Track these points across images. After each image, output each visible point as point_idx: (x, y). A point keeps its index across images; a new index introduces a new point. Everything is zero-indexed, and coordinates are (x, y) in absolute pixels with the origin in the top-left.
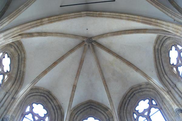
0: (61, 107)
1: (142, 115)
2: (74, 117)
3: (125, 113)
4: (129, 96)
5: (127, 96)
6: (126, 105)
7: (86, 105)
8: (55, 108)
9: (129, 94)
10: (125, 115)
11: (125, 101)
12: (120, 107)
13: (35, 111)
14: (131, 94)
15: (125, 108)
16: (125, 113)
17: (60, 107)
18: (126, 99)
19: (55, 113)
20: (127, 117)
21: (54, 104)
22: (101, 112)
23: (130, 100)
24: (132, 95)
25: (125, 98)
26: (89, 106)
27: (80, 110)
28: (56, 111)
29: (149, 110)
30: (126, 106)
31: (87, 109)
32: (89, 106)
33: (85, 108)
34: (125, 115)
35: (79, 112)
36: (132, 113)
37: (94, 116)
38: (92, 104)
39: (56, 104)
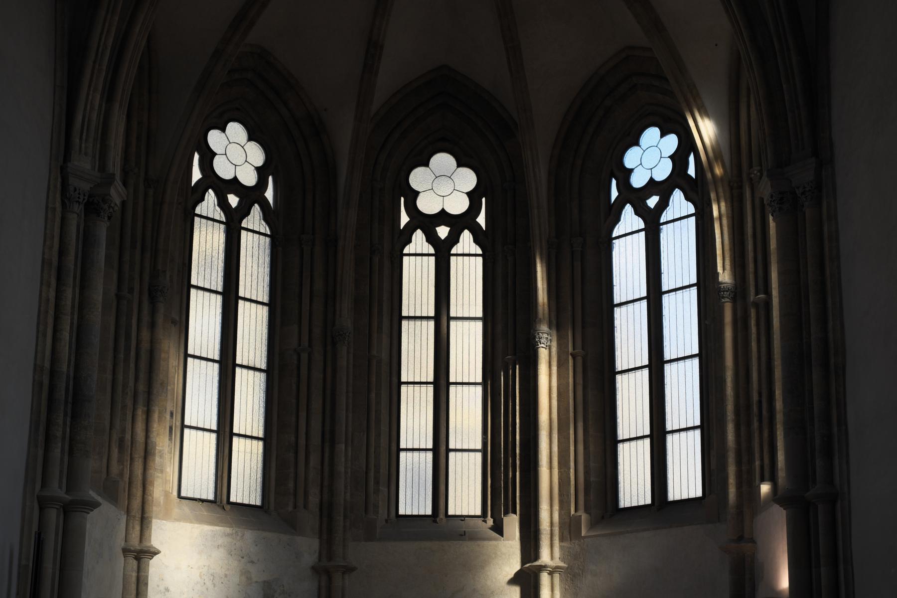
13: (223, 169)
29: (663, 189)
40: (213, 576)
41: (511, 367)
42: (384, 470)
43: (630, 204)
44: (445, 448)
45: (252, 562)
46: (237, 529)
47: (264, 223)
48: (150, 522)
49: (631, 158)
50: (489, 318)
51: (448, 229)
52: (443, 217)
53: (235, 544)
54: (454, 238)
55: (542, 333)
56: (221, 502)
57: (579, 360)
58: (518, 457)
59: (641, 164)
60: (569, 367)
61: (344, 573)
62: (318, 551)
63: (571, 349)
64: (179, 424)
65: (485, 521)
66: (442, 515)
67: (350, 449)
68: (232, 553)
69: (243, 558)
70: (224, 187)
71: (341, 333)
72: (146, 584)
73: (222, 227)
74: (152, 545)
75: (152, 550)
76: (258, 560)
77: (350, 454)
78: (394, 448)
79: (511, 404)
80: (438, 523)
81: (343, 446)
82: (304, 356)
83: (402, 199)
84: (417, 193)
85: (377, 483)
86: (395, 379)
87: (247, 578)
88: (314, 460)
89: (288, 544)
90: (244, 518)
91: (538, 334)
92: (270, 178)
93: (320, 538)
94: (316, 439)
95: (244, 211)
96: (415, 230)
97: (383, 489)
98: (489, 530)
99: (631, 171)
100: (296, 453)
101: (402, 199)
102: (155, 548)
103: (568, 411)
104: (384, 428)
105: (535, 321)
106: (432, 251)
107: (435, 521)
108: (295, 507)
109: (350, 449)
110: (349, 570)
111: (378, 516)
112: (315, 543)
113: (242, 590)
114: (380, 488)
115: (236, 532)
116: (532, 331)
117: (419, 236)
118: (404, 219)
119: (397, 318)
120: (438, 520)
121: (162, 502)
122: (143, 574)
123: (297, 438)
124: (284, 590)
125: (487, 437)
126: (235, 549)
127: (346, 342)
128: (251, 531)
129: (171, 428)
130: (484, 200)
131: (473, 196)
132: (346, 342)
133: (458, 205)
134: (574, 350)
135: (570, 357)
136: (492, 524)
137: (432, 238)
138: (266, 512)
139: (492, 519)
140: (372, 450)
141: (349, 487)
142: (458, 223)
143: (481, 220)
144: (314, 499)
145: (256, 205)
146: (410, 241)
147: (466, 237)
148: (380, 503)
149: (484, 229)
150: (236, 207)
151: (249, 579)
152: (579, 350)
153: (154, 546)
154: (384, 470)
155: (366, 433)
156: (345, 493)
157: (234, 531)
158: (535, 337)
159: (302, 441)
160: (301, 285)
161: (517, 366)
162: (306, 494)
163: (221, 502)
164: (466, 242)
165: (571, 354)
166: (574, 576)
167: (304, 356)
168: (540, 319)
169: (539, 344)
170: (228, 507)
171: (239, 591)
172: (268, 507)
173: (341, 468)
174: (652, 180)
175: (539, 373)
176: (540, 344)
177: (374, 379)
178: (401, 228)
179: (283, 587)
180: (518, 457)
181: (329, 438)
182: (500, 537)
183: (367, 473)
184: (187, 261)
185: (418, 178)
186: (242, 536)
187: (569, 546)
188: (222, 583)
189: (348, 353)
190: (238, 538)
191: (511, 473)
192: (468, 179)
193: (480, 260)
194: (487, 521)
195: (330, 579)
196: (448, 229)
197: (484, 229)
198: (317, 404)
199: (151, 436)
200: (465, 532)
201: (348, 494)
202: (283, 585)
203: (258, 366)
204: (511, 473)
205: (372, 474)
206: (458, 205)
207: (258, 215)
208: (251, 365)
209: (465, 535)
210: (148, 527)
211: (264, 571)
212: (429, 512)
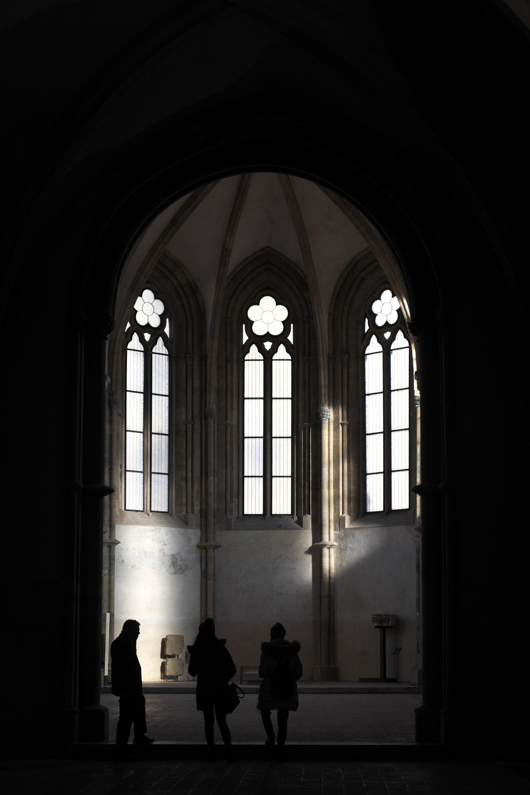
2: (228, 307)
40: (146, 553)
41: (307, 429)
42: (235, 489)
43: (375, 335)
44: (270, 475)
45: (165, 544)
46: (157, 527)
47: (165, 348)
48: (115, 527)
50: (295, 398)
51: (271, 344)
52: (268, 337)
53: (156, 535)
54: (274, 350)
55: (324, 412)
56: (147, 511)
57: (346, 427)
58: (311, 482)
59: (381, 312)
60: (339, 431)
61: (214, 549)
62: (200, 537)
63: (341, 421)
64: (123, 470)
65: (293, 518)
66: (268, 515)
67: (216, 479)
68: (155, 540)
69: (160, 542)
70: (141, 330)
71: (210, 413)
72: (114, 559)
73: (142, 353)
74: (116, 539)
75: (116, 542)
76: (168, 543)
77: (216, 481)
78: (241, 476)
79: (307, 451)
80: (266, 519)
81: (212, 478)
82: (190, 426)
83: (244, 325)
84: (252, 322)
85: (232, 497)
86: (241, 436)
87: (163, 553)
88: (196, 486)
89: (184, 534)
90: (160, 520)
91: (322, 412)
92: (167, 320)
93: (201, 529)
94: (197, 474)
95: (153, 342)
96: (251, 345)
97: (235, 500)
98: (295, 523)
99: (376, 315)
100: (186, 482)
101: (244, 325)
102: (118, 541)
103: (339, 456)
104: (235, 465)
105: (320, 404)
106: (262, 358)
107: (265, 518)
108: (187, 512)
109: (216, 479)
110: (217, 547)
111: (232, 516)
112: (198, 532)
113: (161, 560)
114: (234, 500)
115: (156, 529)
116: (319, 410)
117: (254, 349)
118: (245, 338)
119: (241, 398)
120: (266, 517)
121: (119, 515)
122: (112, 554)
123: (186, 473)
124: (182, 559)
125: (294, 469)
126: (156, 538)
127: (213, 418)
128: (164, 528)
129: (121, 474)
130: (292, 325)
131: (286, 323)
132: (213, 418)
133: (277, 330)
134: (342, 421)
135: (340, 425)
136: (297, 519)
137: (261, 350)
138: (170, 515)
139: (297, 517)
140: (229, 478)
141: (216, 500)
142: (277, 340)
143: (291, 338)
144: (197, 508)
145: (160, 338)
146: (248, 352)
147: (282, 348)
148: (234, 508)
149: (292, 343)
150: (149, 341)
151: (164, 553)
152: (345, 421)
153: (117, 539)
154: (235, 489)
155: (225, 469)
156: (214, 504)
157: (155, 528)
158: (320, 414)
159: (190, 475)
160: (187, 384)
161: (311, 429)
162: (193, 505)
163: (147, 511)
164: (282, 352)
165: (341, 423)
166: (341, 550)
167: (190, 426)
168: (323, 403)
169: (322, 418)
170: (151, 514)
171: (159, 560)
172: (172, 513)
173: (212, 491)
174: (387, 323)
175: (322, 435)
176: (323, 418)
177: (229, 437)
178: (244, 344)
179: (182, 557)
180: (311, 482)
181: (205, 473)
182: (301, 528)
183: (226, 491)
184: (124, 378)
185: (253, 312)
186: (159, 531)
187: (339, 533)
188: (150, 556)
189: (214, 423)
190: (158, 532)
191: (307, 491)
192: (283, 312)
193: (290, 362)
194: (294, 518)
195: (207, 552)
196: (271, 344)
197: (292, 343)
198: (197, 454)
199: (113, 482)
200: (281, 525)
201: (216, 504)
202: (181, 556)
203: (164, 433)
204: (307, 491)
205: (229, 492)
206: (277, 330)
207: (161, 343)
208: (160, 432)
209: (281, 526)
210: (114, 530)
211: (171, 549)
212: (261, 512)
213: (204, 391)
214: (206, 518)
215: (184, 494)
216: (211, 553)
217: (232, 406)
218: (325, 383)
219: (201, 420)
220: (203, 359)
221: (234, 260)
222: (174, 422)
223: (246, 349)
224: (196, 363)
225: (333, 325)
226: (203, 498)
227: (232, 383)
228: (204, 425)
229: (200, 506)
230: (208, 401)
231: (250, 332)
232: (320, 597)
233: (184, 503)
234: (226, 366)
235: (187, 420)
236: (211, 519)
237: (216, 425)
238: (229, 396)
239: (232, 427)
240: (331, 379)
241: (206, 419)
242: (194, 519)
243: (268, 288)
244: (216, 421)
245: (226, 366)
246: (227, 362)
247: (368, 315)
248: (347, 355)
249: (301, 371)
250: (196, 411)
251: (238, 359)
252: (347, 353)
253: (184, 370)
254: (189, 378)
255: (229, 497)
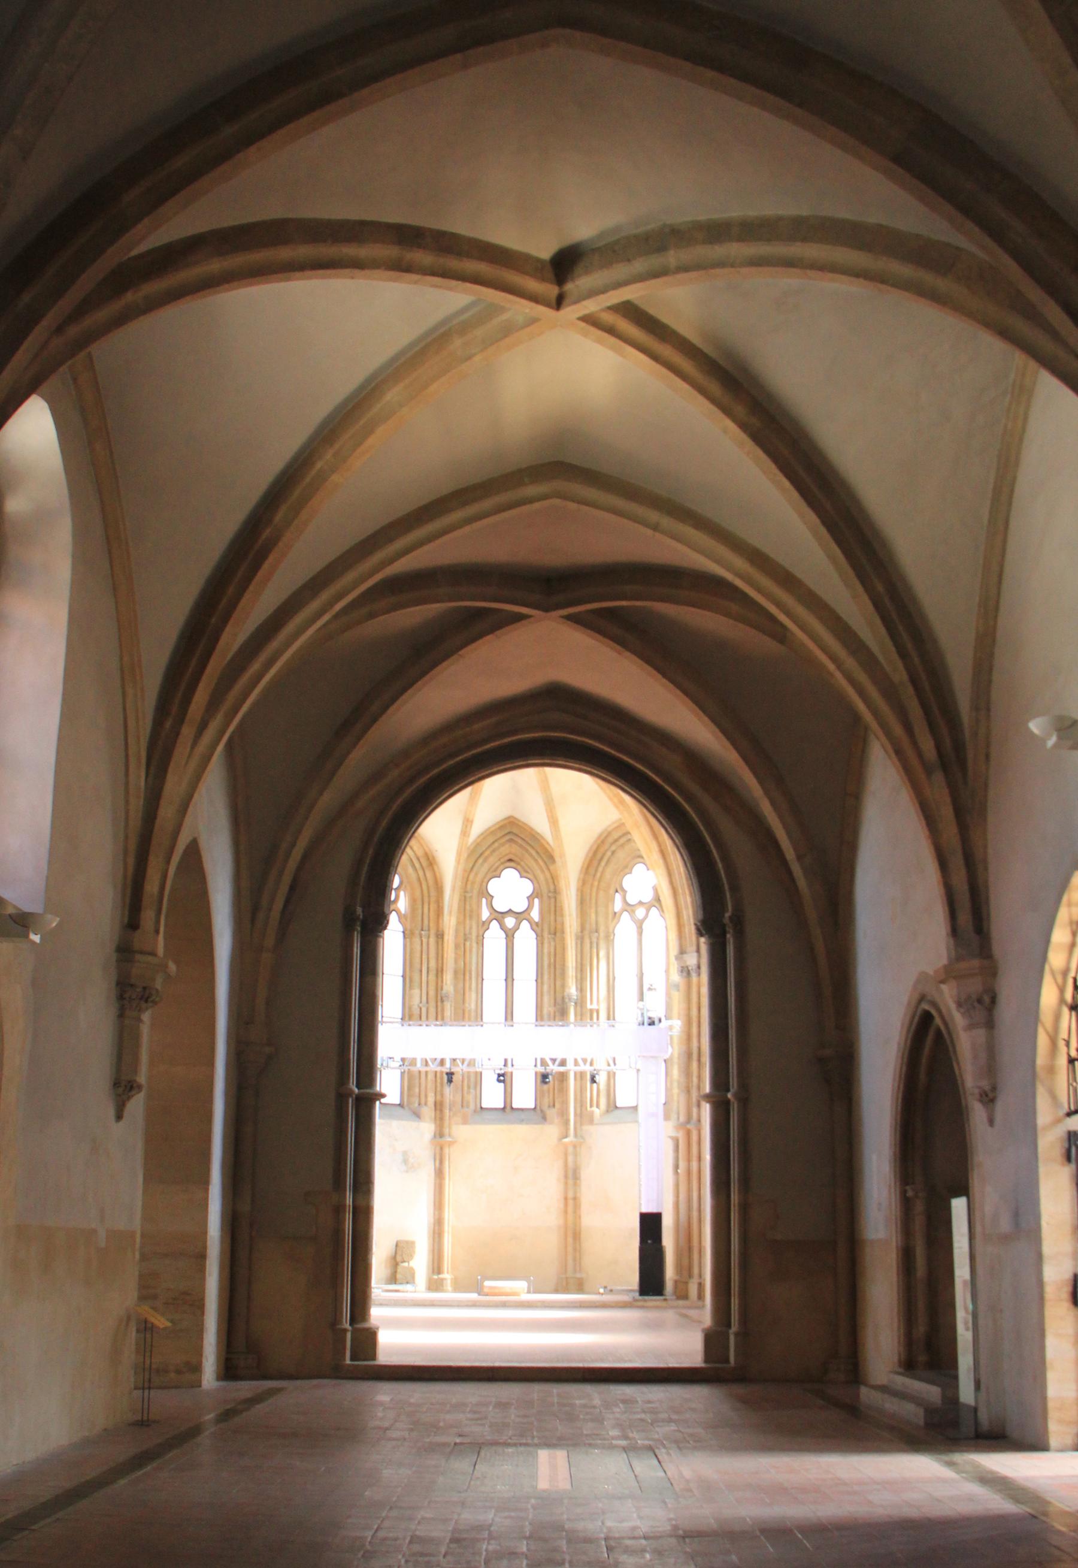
0: (434, 858)
1: (629, 907)
3: (595, 889)
4: (616, 841)
5: (610, 840)
6: (603, 863)
7: (499, 835)
8: (417, 865)
9: (615, 835)
10: (594, 894)
11: (602, 850)
12: (585, 866)
14: (620, 837)
15: (598, 874)
16: (595, 889)
17: (431, 858)
18: (606, 846)
19: (419, 879)
20: (596, 903)
21: (415, 854)
22: (536, 860)
23: (613, 853)
24: (622, 841)
25: (603, 842)
26: (507, 838)
27: (481, 854)
28: (421, 873)
29: (648, 907)
30: (600, 869)
31: (503, 845)
32: (507, 838)
33: (496, 845)
34: (594, 894)
35: (480, 861)
36: (612, 891)
37: (519, 867)
38: (515, 831)
39: (420, 853)
49: (628, 882)
54: (517, 928)
66: (508, 1107)
85: (469, 1087)
93: (435, 1123)
97: (472, 1091)
118: (485, 914)
131: (530, 898)
137: (502, 927)
142: (520, 916)
143: (535, 915)
144: (431, 1100)
147: (525, 925)
156: (450, 1095)
160: (421, 964)
162: (426, 1096)
183: (463, 1082)
185: (493, 886)
189: (451, 1006)
206: (520, 906)
213: (440, 972)
214: (441, 1111)
215: (417, 1085)
216: (446, 1150)
217: (470, 988)
218: (572, 964)
219: (437, 1002)
220: (440, 936)
221: (476, 830)
222: (407, 1005)
223: (486, 925)
224: (432, 940)
225: (582, 902)
226: (438, 1089)
227: (471, 963)
228: (439, 1009)
229: (434, 1098)
230: (444, 981)
231: (491, 906)
232: (566, 1199)
233: (417, 1095)
234: (464, 944)
235: (421, 1002)
236: (447, 1112)
237: (453, 1008)
238: (467, 977)
239: (470, 1011)
240: (579, 960)
241: (442, 1001)
242: (428, 1111)
243: (510, 860)
244: (453, 1005)
245: (464, 944)
246: (465, 940)
247: (619, 890)
248: (596, 934)
249: (546, 951)
250: (432, 993)
251: (478, 936)
252: (597, 932)
253: (418, 948)
254: (425, 957)
255: (466, 1088)
